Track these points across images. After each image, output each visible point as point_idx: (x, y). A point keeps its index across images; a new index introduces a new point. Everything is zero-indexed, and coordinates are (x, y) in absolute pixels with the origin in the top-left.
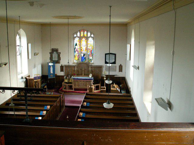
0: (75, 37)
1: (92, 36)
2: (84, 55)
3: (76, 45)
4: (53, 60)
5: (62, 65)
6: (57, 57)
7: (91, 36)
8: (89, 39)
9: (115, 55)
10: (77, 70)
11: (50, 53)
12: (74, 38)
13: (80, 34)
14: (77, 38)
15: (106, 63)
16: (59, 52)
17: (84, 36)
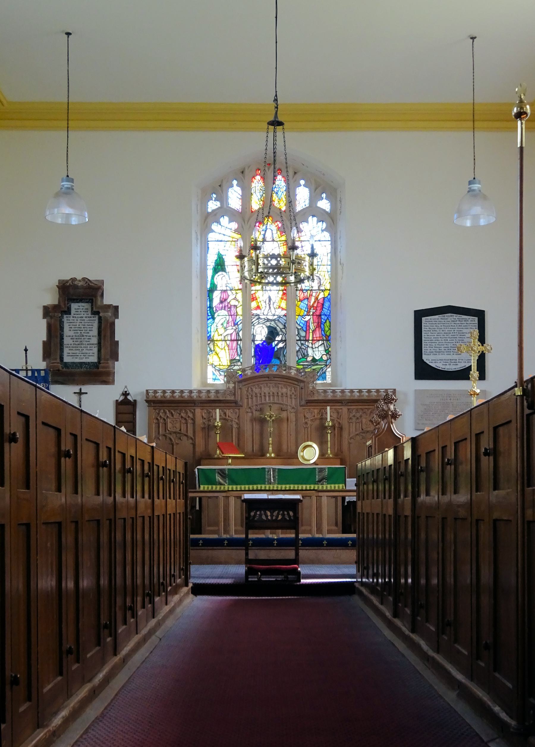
0: (215, 217)
1: (324, 204)
2: (272, 333)
3: (220, 266)
4: (67, 359)
5: (126, 394)
6: (95, 340)
7: (312, 210)
8: (303, 226)
9: (480, 315)
10: (226, 429)
11: (47, 311)
12: (208, 220)
13: (246, 197)
14: (225, 220)
15: (424, 371)
16: (107, 300)
17: (268, 210)
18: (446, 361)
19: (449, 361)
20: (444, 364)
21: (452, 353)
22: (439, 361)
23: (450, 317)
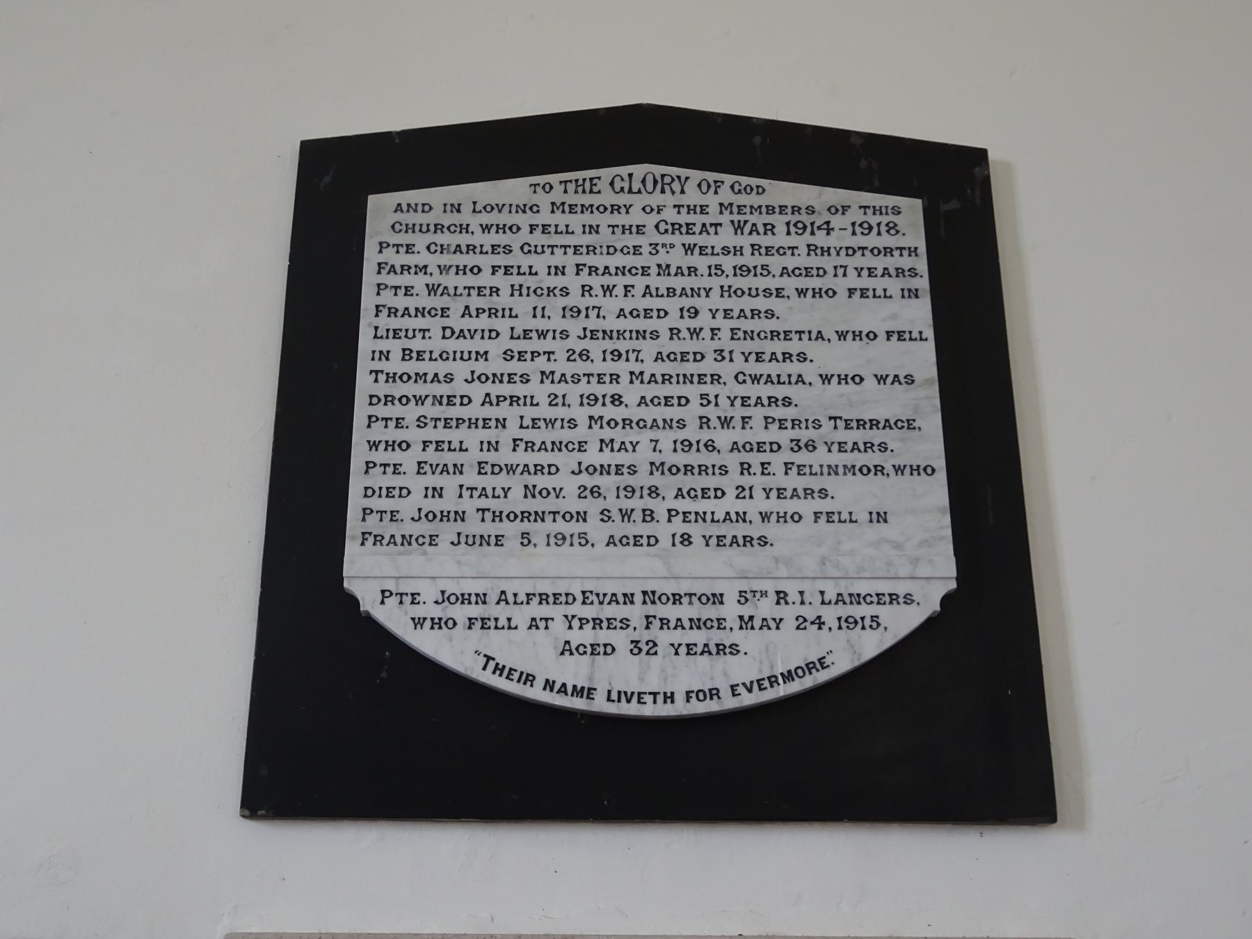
18: (598, 617)
19: (636, 613)
20: (587, 636)
21: (663, 530)
22: (522, 616)
23: (636, 194)
